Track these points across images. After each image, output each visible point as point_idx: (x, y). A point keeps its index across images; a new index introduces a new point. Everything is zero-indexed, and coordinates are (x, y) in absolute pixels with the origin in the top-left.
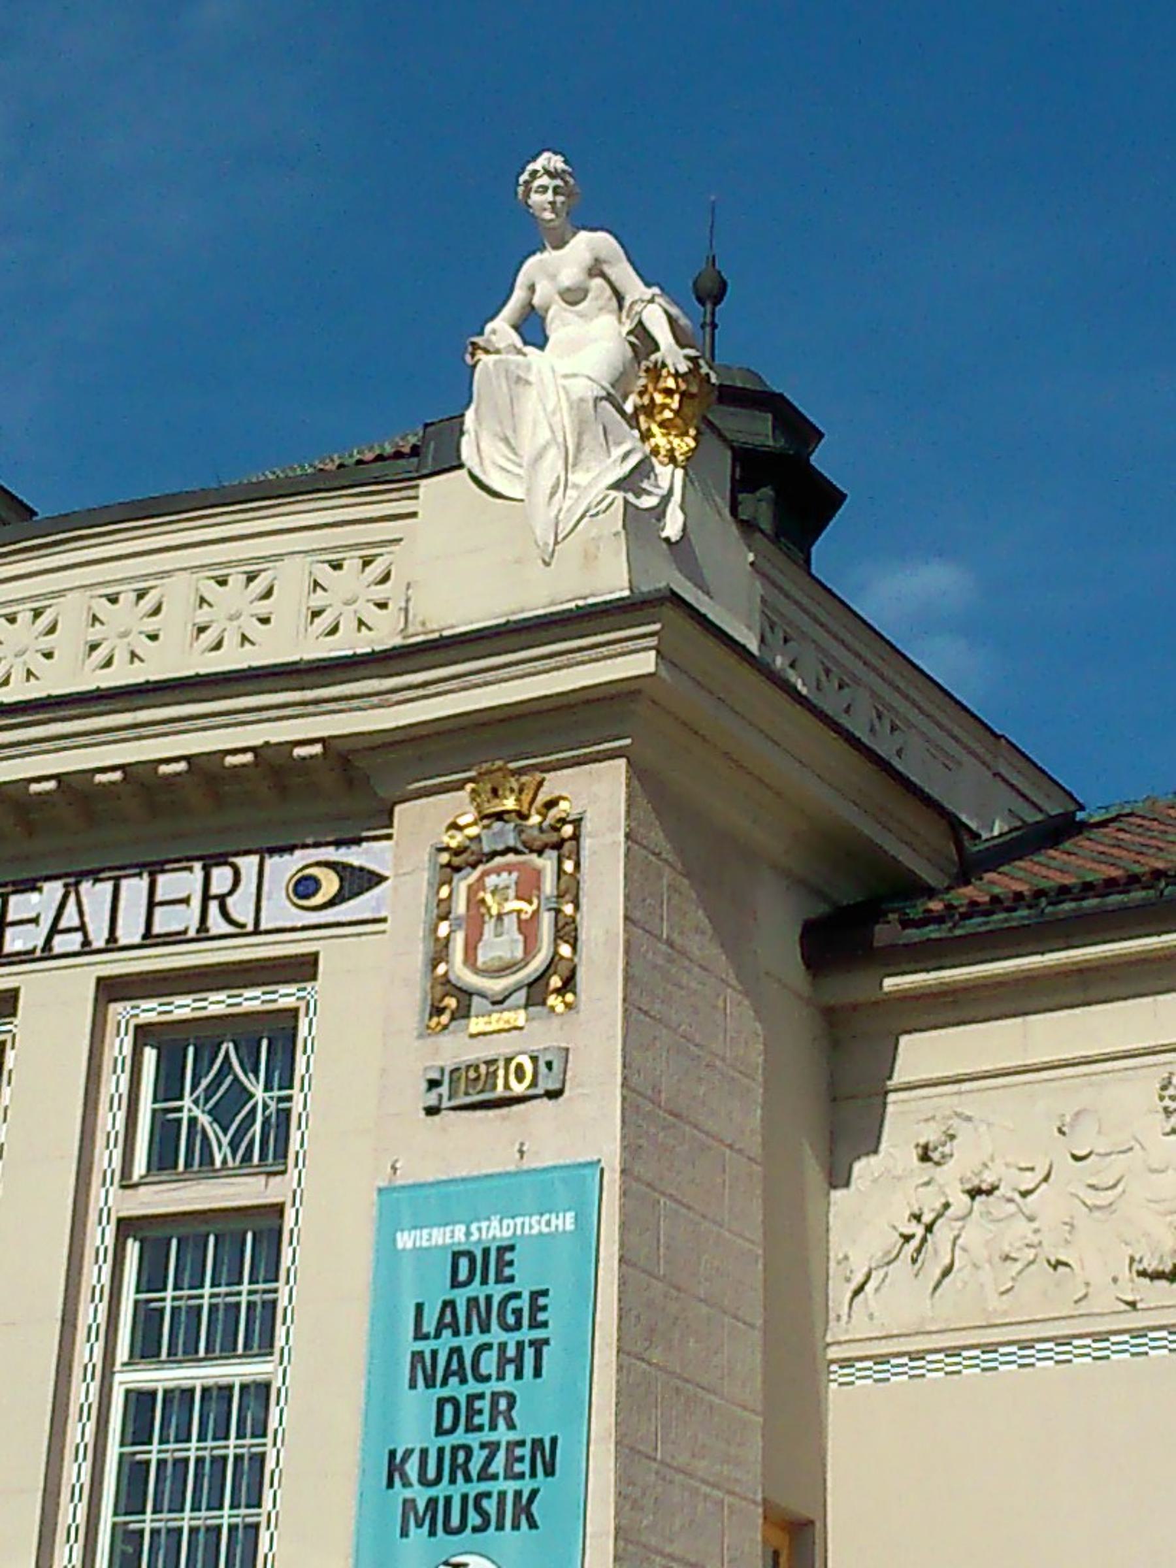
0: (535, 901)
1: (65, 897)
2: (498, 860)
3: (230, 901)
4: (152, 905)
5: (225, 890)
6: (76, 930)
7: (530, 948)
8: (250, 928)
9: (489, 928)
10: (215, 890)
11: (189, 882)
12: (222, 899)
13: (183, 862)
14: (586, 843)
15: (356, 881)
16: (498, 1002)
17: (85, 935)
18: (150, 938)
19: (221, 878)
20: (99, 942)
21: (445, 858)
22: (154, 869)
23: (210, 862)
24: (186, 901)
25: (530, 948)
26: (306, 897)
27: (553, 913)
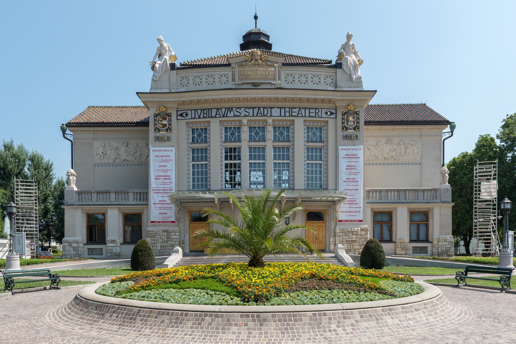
7: (354, 124)
11: (314, 111)
13: (313, 109)
14: (360, 114)
15: (332, 114)
16: (350, 129)
19: (317, 111)
22: (310, 109)
25: (354, 124)
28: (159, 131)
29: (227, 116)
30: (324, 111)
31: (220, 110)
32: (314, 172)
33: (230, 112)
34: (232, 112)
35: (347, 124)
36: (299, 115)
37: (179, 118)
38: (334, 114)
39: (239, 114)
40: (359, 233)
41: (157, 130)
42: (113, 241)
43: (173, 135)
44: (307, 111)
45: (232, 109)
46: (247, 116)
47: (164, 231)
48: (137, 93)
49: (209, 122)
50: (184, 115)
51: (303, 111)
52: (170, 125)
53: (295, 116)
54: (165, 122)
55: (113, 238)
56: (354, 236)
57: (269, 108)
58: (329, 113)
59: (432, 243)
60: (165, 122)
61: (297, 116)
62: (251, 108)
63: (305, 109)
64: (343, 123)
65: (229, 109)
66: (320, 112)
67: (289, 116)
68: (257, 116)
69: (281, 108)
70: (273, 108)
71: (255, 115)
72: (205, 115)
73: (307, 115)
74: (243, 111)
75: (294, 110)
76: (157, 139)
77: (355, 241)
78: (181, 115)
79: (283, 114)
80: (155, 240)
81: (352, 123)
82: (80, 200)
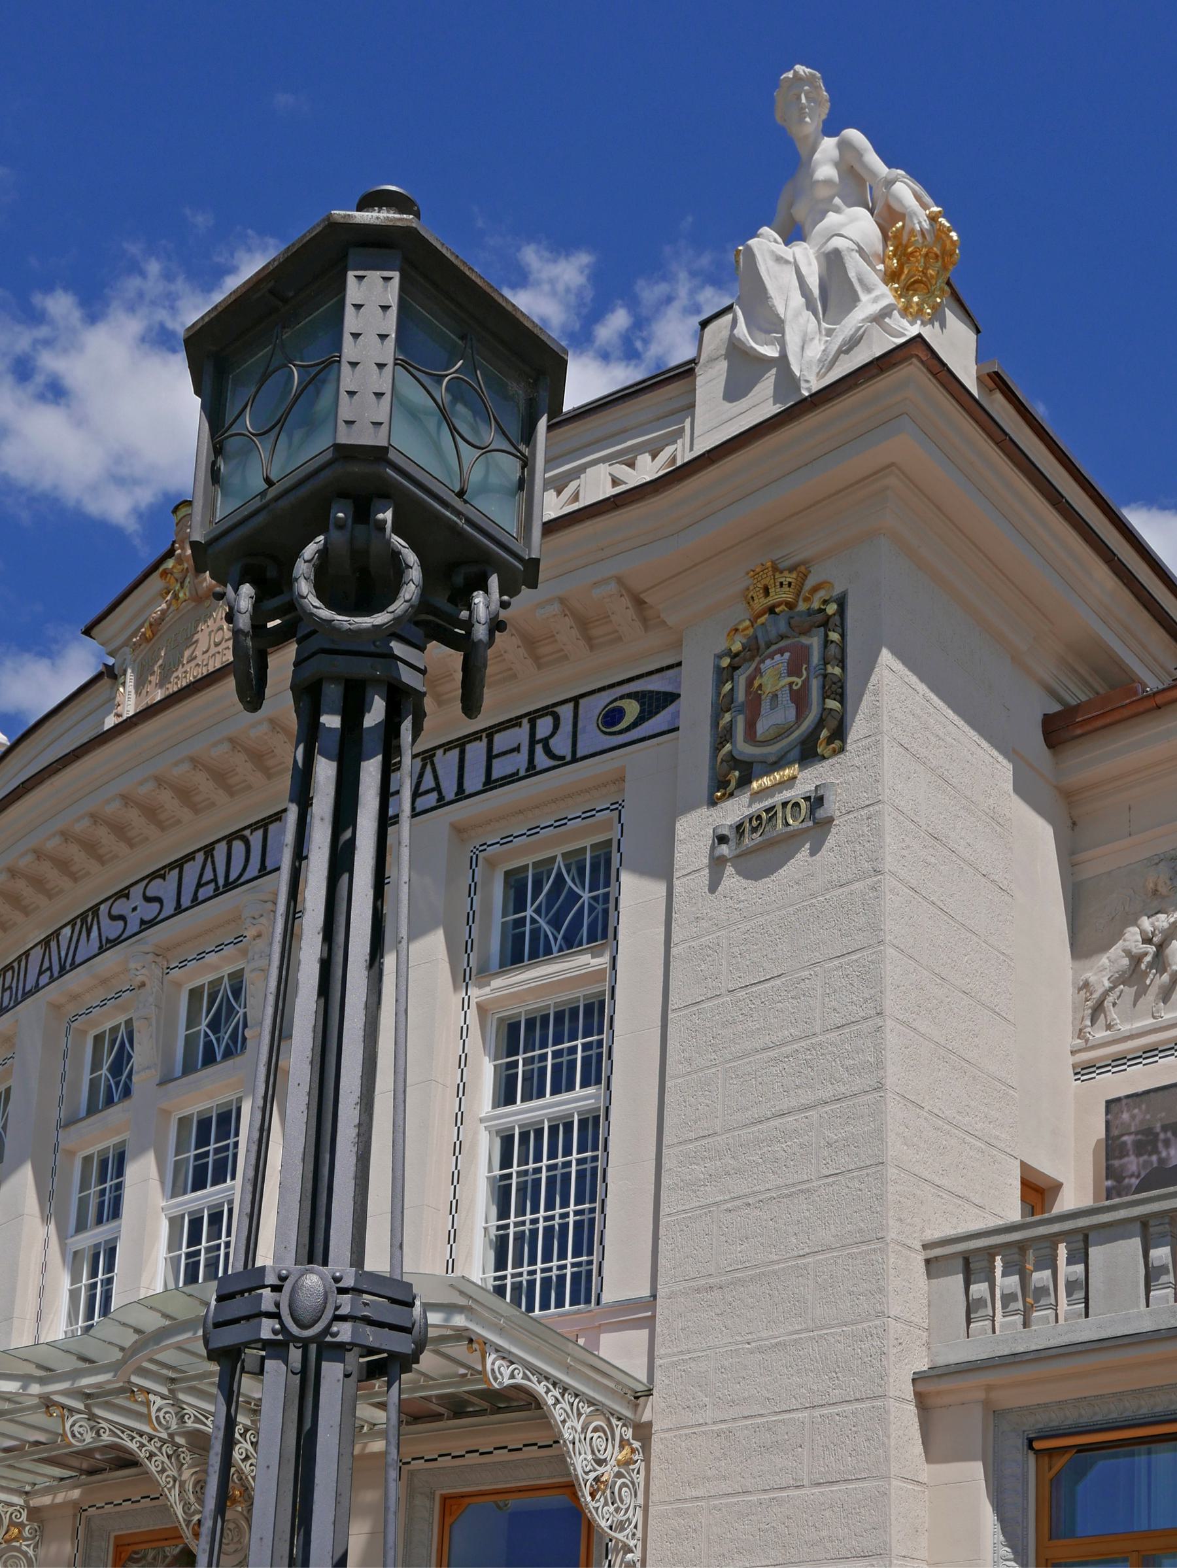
0: (804, 673)
1: (424, 767)
2: (774, 648)
3: (552, 742)
4: (490, 757)
5: (548, 733)
6: (432, 790)
8: (568, 758)
9: (765, 706)
10: (539, 736)
11: (521, 735)
12: (545, 742)
13: (514, 722)
17: (440, 793)
18: (490, 784)
19: (544, 726)
20: (450, 794)
21: (726, 662)
24: (517, 749)
26: (613, 724)
27: (820, 678)
29: (74, 966)
30: (593, 708)
34: (94, 933)
35: (751, 735)
44: (476, 752)
45: (95, 909)
58: (632, 709)
62: (171, 866)
64: (723, 736)
65: (83, 916)
68: (196, 902)
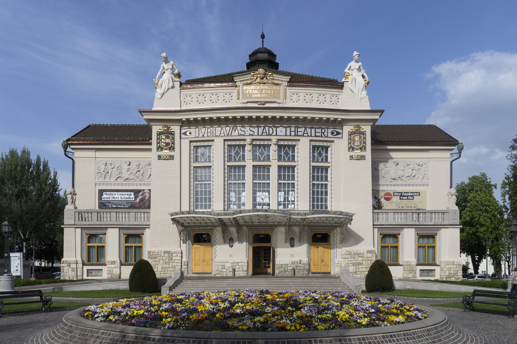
11: (320, 130)
13: (319, 128)
15: (338, 133)
16: (357, 149)
18: (315, 136)
19: (323, 131)
23: (322, 129)
28: (162, 149)
31: (224, 128)
32: (320, 193)
33: (235, 131)
36: (305, 135)
37: (183, 136)
38: (340, 133)
39: (243, 133)
40: (365, 256)
41: (160, 148)
42: (113, 262)
43: (176, 153)
46: (252, 135)
47: (165, 252)
48: (141, 112)
49: (213, 141)
50: (188, 133)
51: (309, 130)
52: (173, 143)
53: (300, 136)
54: (168, 141)
55: (113, 259)
56: (360, 259)
57: (274, 127)
58: (335, 133)
59: (439, 266)
60: (168, 141)
61: (303, 136)
63: (311, 128)
64: (350, 143)
66: (326, 132)
67: (295, 135)
68: (262, 135)
69: (286, 128)
70: (278, 127)
71: (260, 134)
72: (209, 134)
73: (313, 135)
74: (248, 130)
75: (299, 130)
76: (159, 157)
77: (362, 264)
78: (185, 134)
79: (288, 134)
80: (156, 261)
81: (358, 144)
82: (80, 220)
